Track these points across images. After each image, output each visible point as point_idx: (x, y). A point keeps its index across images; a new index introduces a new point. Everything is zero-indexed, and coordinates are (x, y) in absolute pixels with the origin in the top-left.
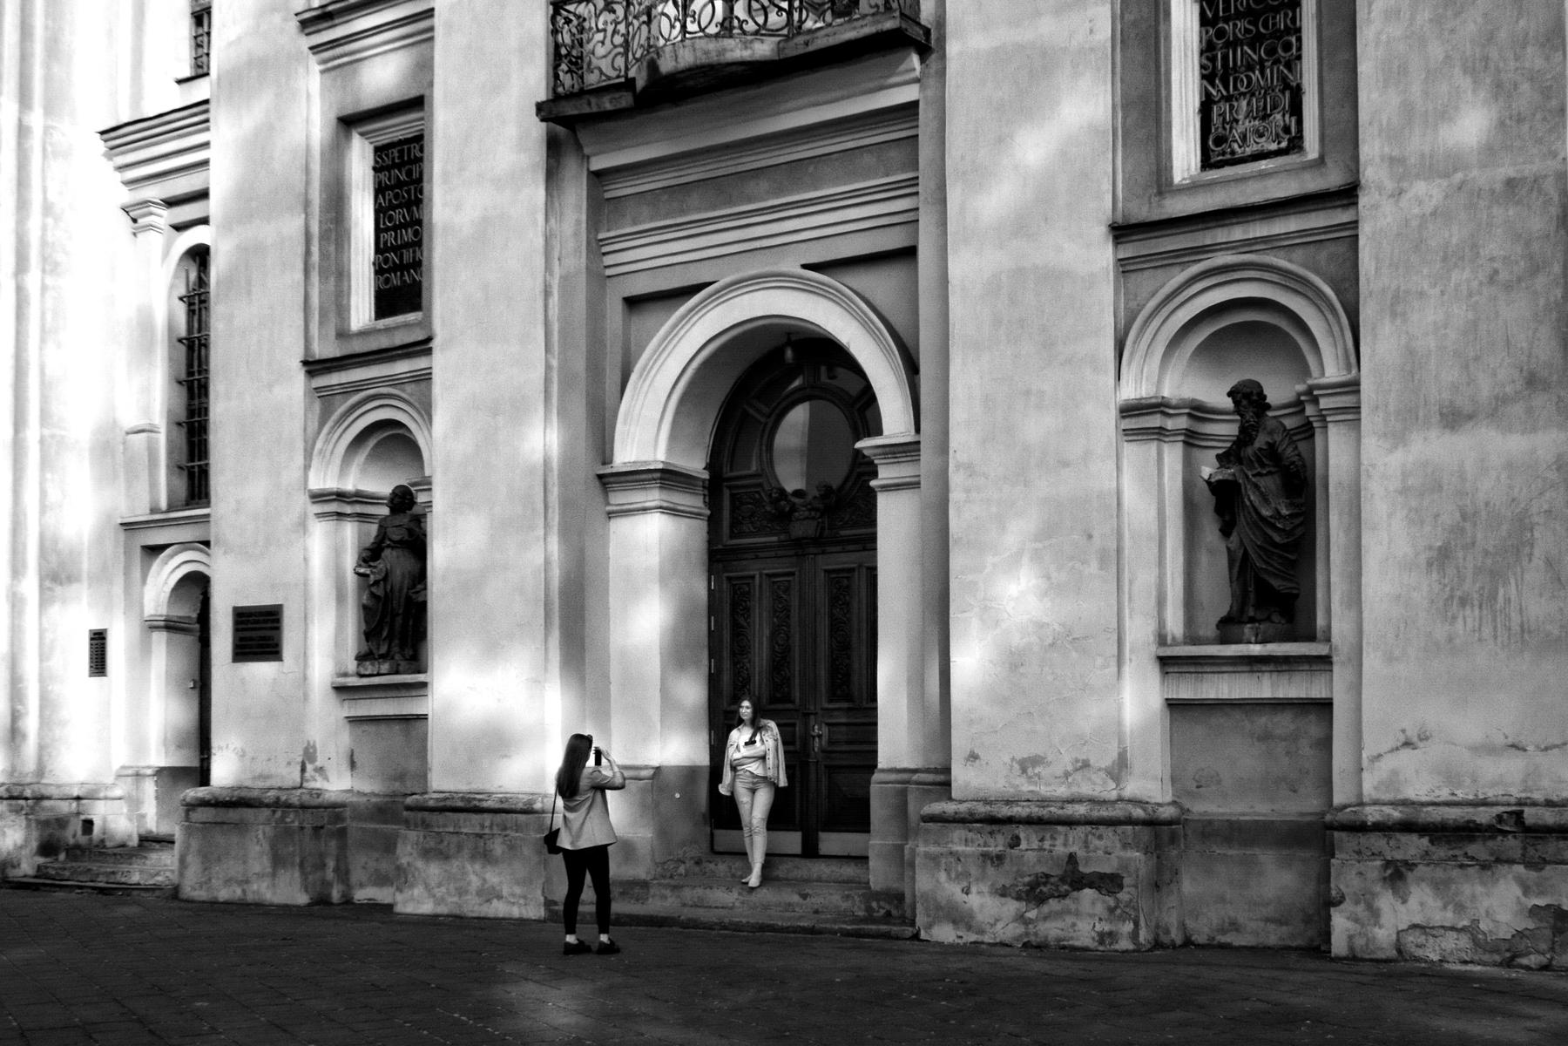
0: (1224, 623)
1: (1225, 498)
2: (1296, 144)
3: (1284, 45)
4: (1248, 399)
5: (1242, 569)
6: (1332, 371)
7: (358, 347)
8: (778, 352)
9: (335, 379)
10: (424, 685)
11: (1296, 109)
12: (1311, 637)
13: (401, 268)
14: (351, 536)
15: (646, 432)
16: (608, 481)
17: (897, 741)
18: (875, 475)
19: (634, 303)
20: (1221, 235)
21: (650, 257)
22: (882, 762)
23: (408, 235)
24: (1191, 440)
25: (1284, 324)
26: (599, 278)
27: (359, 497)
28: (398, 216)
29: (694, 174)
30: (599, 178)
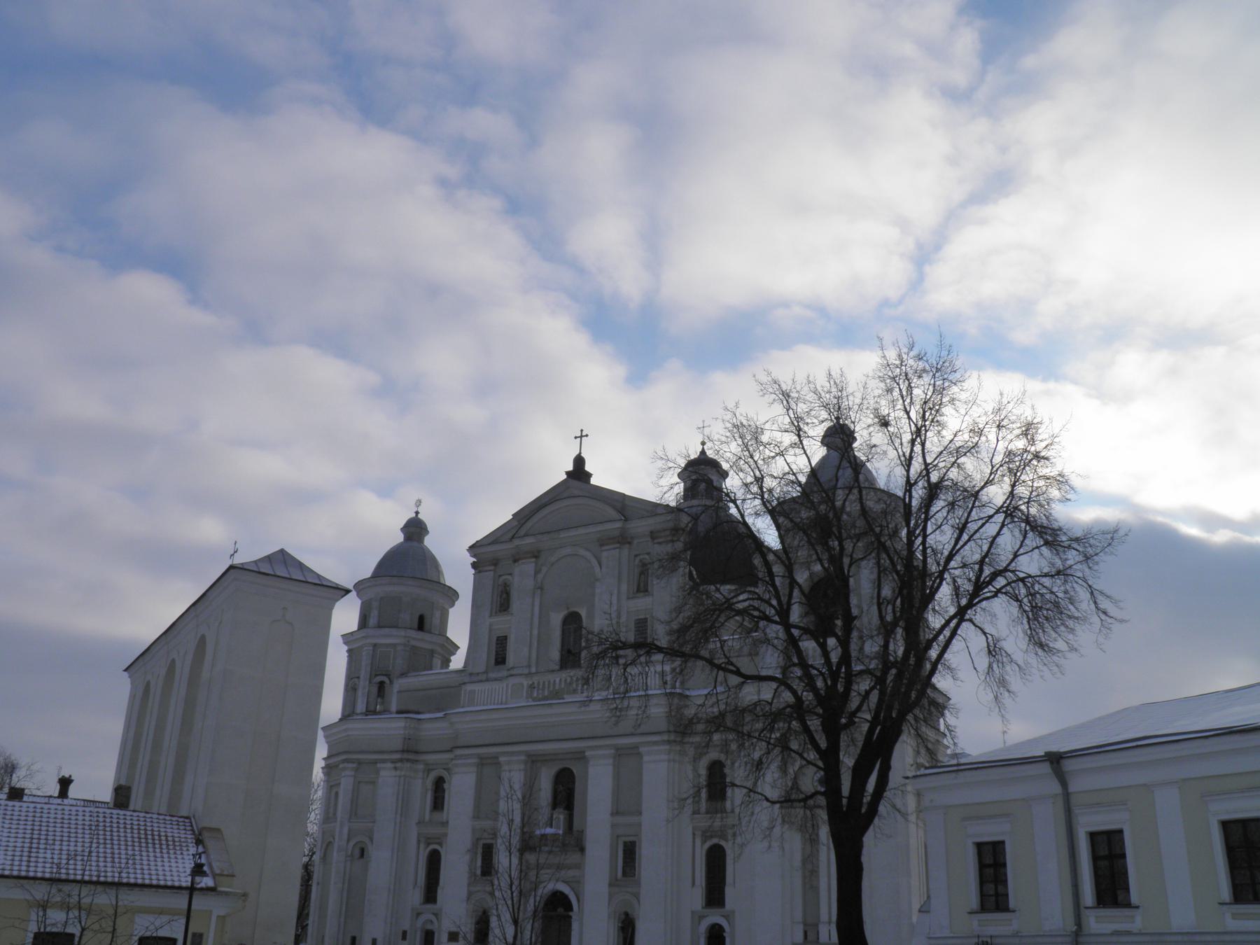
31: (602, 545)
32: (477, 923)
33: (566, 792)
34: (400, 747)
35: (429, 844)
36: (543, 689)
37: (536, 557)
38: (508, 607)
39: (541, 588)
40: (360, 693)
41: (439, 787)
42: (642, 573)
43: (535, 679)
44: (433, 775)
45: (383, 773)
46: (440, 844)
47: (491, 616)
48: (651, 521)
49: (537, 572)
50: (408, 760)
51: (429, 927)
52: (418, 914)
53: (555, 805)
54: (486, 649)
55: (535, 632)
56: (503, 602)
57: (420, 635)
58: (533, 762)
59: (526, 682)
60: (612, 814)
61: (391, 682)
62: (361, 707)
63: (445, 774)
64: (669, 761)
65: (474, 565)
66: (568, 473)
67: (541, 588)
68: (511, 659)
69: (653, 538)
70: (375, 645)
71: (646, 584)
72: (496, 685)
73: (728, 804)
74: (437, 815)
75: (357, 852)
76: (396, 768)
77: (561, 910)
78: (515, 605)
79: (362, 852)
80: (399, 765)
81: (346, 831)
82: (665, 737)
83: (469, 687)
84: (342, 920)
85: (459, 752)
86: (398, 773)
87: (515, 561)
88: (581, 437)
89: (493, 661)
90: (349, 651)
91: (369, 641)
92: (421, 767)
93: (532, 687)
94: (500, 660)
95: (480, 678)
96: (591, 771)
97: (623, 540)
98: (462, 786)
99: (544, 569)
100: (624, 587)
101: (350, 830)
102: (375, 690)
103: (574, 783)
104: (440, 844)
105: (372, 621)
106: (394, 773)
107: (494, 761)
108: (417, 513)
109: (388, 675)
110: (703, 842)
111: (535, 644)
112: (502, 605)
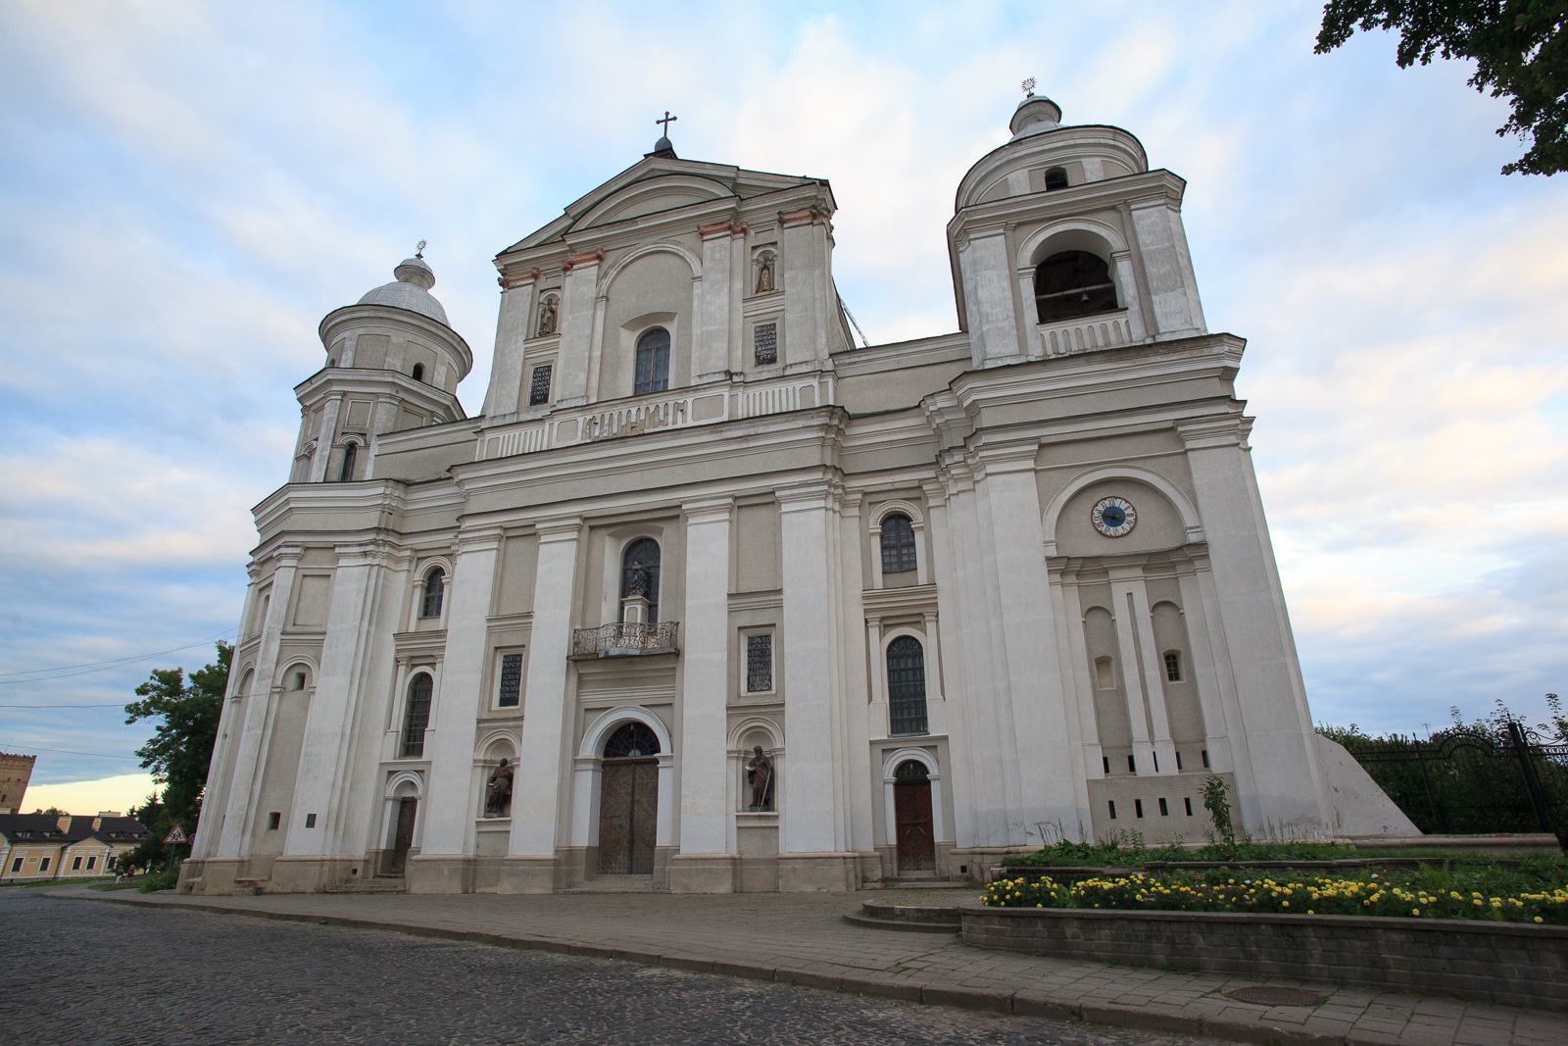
0: (751, 806)
1: (751, 774)
2: (770, 689)
3: (767, 665)
4: (758, 751)
5: (757, 795)
6: (779, 745)
7: (495, 716)
8: (629, 725)
9: (487, 725)
10: (510, 821)
11: (770, 680)
12: (773, 810)
13: (510, 692)
14: (487, 774)
15: (590, 748)
16: (576, 761)
17: (663, 839)
18: (658, 763)
19: (586, 710)
20: (753, 711)
21: (594, 697)
22: (657, 845)
23: (513, 683)
24: (744, 759)
25: (764, 731)
26: (578, 702)
27: (491, 761)
28: (510, 677)
29: (609, 677)
30: (580, 676)
31: (702, 234)
32: (493, 779)
33: (642, 570)
34: (375, 525)
35: (414, 666)
36: (610, 424)
37: (599, 258)
38: (554, 329)
39: (607, 300)
40: (316, 457)
41: (434, 582)
42: (766, 267)
43: (597, 413)
44: (425, 565)
45: (342, 562)
46: (433, 665)
47: (526, 341)
48: (780, 199)
49: (600, 278)
50: (385, 543)
51: (408, 794)
52: (391, 773)
53: (625, 591)
54: (518, 383)
55: (597, 353)
56: (547, 325)
57: (415, 386)
58: (592, 528)
59: (581, 419)
60: (730, 596)
61: (367, 446)
62: (317, 474)
63: (444, 563)
64: (827, 509)
65: (502, 283)
66: (646, 156)
67: (607, 300)
68: (557, 391)
69: (782, 222)
70: (344, 394)
71: (771, 282)
72: (532, 430)
73: (922, 577)
74: (430, 625)
75: (293, 680)
76: (365, 554)
77: (635, 754)
78: (565, 323)
79: (302, 678)
80: (370, 548)
81: (275, 647)
82: (818, 476)
83: (489, 436)
84: (258, 787)
85: (468, 523)
86: (369, 561)
87: (566, 269)
88: (667, 120)
89: (528, 400)
90: (305, 409)
91: (334, 388)
92: (408, 553)
93: (592, 422)
94: (539, 397)
95: (508, 420)
96: (693, 532)
97: (735, 226)
98: (473, 576)
99: (613, 273)
100: (738, 285)
101: (281, 646)
102: (340, 455)
103: (658, 558)
104: (433, 665)
105: (346, 361)
106: (362, 561)
107: (530, 534)
108: (419, 256)
109: (362, 435)
110: (882, 635)
111: (596, 368)
112: (543, 325)
